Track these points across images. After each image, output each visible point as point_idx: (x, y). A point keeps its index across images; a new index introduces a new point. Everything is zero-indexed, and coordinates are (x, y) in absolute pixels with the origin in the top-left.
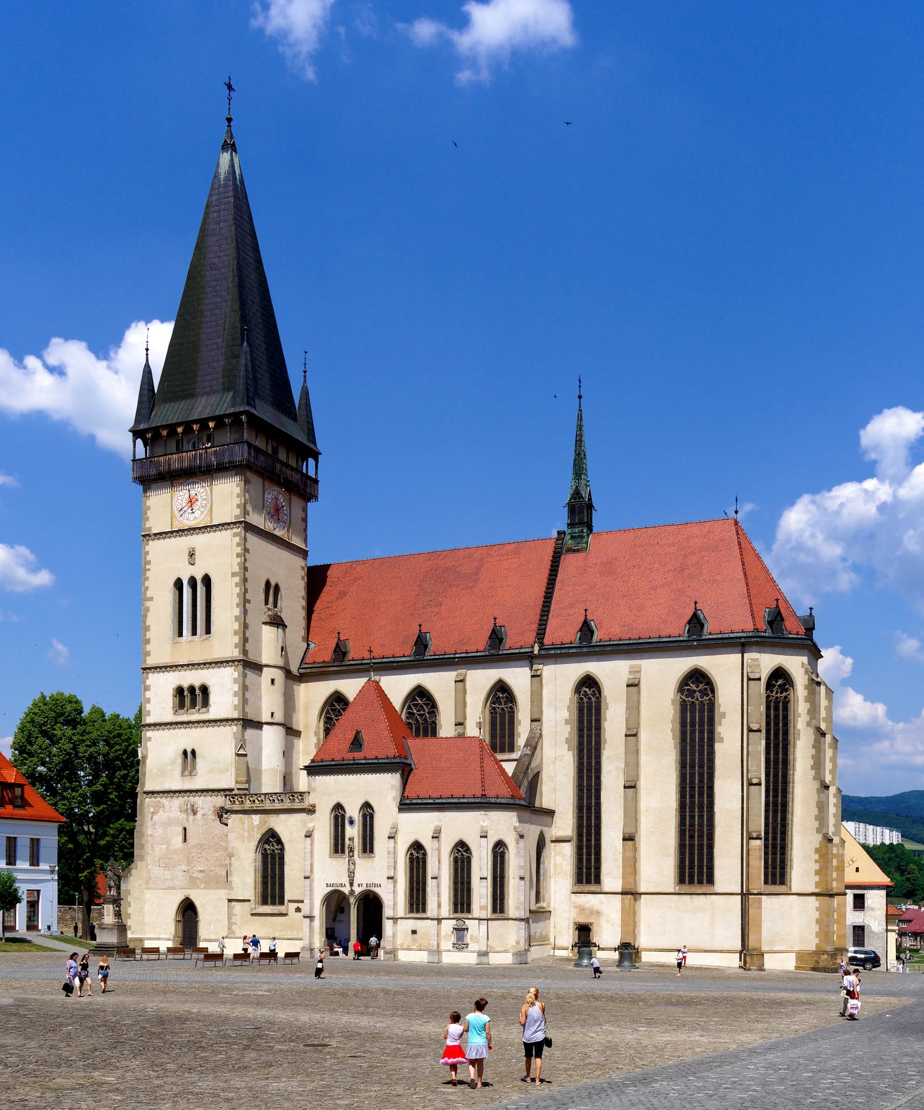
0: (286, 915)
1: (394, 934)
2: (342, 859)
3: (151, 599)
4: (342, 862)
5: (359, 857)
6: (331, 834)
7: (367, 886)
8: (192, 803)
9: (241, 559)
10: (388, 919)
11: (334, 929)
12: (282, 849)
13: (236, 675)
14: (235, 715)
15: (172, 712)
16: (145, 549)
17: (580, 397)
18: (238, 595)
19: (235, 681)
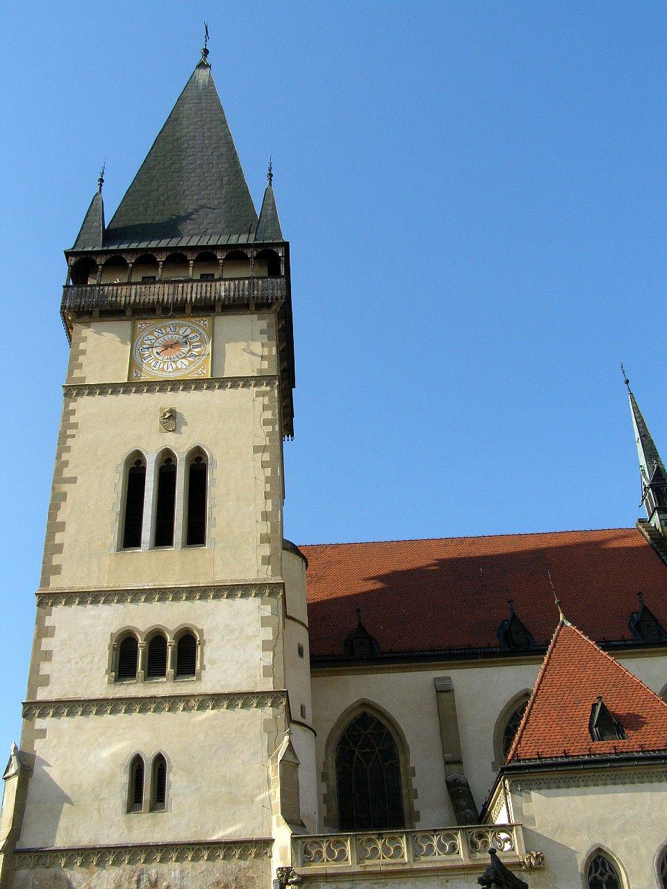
3: (73, 480)
8: (153, 879)
9: (274, 428)
13: (267, 610)
14: (268, 686)
15: (106, 679)
16: (67, 406)
17: (627, 382)
18: (267, 480)
19: (265, 622)
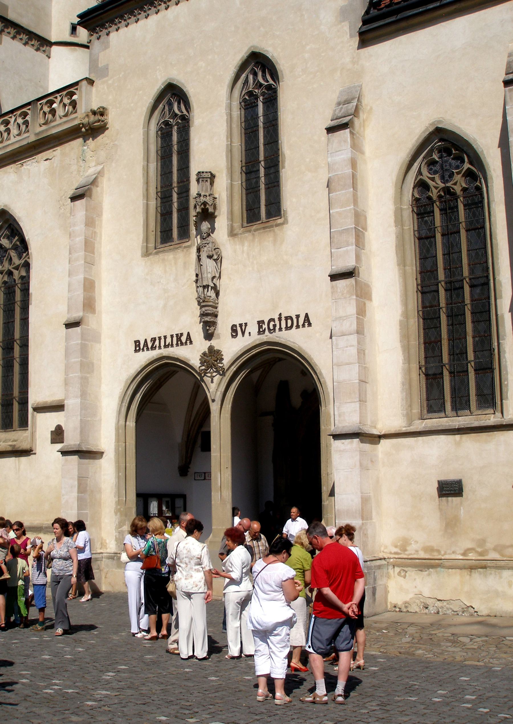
0: (27, 452)
1: (365, 500)
2: (180, 254)
4: (180, 262)
5: (232, 234)
6: (147, 183)
7: (261, 332)
10: (337, 437)
11: (184, 497)
12: (27, 266)
